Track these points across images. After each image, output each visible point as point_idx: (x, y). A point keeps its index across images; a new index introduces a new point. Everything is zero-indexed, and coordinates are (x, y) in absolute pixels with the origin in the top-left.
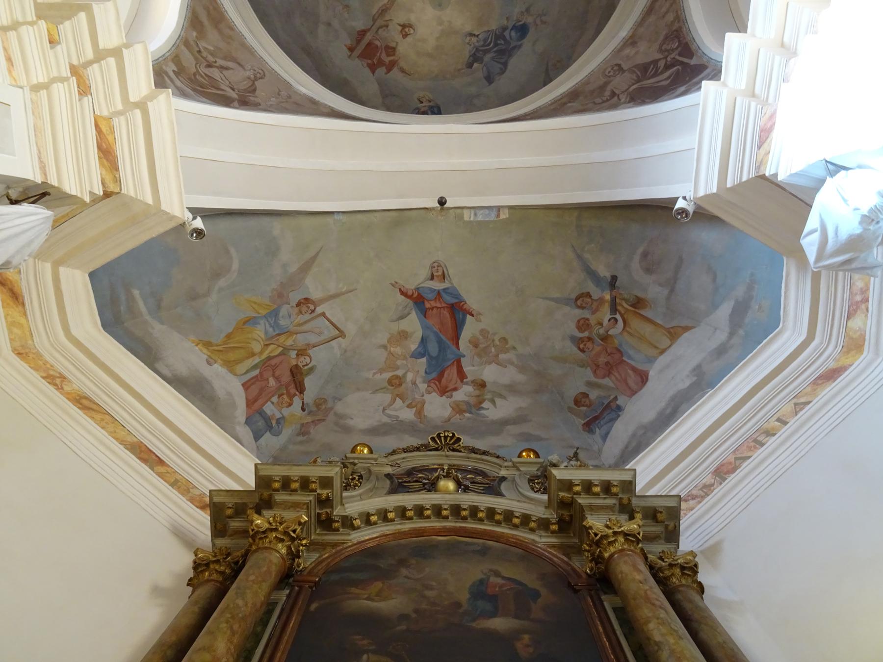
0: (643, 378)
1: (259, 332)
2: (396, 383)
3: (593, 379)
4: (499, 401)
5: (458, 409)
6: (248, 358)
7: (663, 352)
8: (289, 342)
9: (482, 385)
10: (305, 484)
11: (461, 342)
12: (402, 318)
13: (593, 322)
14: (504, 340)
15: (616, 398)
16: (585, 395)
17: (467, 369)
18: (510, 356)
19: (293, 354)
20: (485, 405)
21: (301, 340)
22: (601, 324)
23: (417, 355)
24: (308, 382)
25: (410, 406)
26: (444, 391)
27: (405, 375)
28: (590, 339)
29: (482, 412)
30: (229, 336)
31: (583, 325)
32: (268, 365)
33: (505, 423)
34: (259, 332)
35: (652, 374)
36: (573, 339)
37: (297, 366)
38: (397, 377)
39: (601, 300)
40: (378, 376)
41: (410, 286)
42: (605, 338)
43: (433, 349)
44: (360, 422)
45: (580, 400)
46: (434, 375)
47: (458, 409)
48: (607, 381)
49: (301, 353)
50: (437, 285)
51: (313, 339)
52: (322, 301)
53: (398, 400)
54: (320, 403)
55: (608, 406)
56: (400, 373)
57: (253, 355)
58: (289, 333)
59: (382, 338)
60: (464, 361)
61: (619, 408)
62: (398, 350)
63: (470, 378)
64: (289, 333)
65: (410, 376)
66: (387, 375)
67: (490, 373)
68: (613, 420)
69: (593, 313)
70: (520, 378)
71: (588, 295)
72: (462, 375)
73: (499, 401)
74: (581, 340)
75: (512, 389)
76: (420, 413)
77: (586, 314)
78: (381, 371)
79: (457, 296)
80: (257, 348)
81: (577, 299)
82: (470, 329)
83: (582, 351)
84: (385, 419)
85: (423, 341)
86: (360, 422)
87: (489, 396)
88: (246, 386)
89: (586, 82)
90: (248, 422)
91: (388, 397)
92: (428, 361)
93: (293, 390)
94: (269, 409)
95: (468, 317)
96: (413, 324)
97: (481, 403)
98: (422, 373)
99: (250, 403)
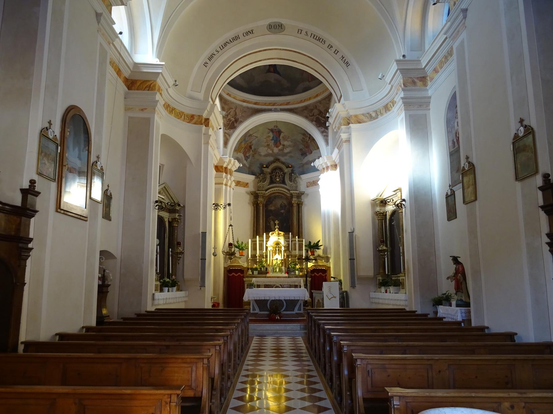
0: (311, 153)
1: (243, 144)
2: (268, 145)
3: (304, 147)
4: (287, 148)
5: (280, 150)
6: (242, 149)
7: (316, 150)
8: (248, 142)
9: (284, 145)
10: (262, 193)
11: (281, 136)
12: (269, 133)
13: (306, 139)
14: (289, 137)
15: (307, 153)
16: (302, 150)
17: (281, 142)
18: (290, 139)
19: (249, 144)
20: (285, 149)
21: (250, 141)
22: (306, 140)
23: (272, 140)
24: (252, 147)
25: (271, 150)
26: (277, 147)
27: (270, 144)
28: (304, 141)
29: (284, 151)
30: (239, 147)
31: (303, 138)
32: (246, 148)
33: (288, 153)
34: (243, 144)
35: (313, 152)
36: (301, 140)
37: (250, 145)
38: (268, 144)
39: (307, 136)
40: (265, 144)
41: (270, 128)
42: (307, 142)
43: (275, 139)
44: (263, 154)
45: (301, 150)
46: (275, 144)
47: (280, 150)
48: (306, 149)
49: (251, 143)
50: (275, 128)
51: (252, 140)
52: (252, 134)
53: (269, 149)
54: (255, 149)
55: (305, 153)
56: (269, 143)
57: (243, 147)
58: (248, 141)
59: (265, 137)
60: (281, 141)
61: (307, 155)
62: (268, 139)
63: (282, 144)
64: (248, 141)
65: (271, 144)
66: (267, 144)
67: (286, 143)
68: (306, 156)
69: (306, 137)
70: (291, 144)
71: (305, 134)
72: (280, 143)
73: (287, 148)
74: (303, 141)
75: (289, 146)
76: (273, 151)
77: (304, 137)
78: (265, 143)
79: (279, 129)
80: (243, 146)
81: (303, 134)
82: (282, 135)
83: (303, 142)
84: (267, 153)
85: (273, 137)
86: (263, 154)
87: (285, 148)
88: (243, 154)
89: (309, 105)
90: (245, 160)
91: (266, 148)
92: (274, 141)
93: (250, 149)
94: (247, 155)
95: (282, 133)
96: (271, 134)
97: (283, 149)
98: (273, 143)
99: (244, 156)
